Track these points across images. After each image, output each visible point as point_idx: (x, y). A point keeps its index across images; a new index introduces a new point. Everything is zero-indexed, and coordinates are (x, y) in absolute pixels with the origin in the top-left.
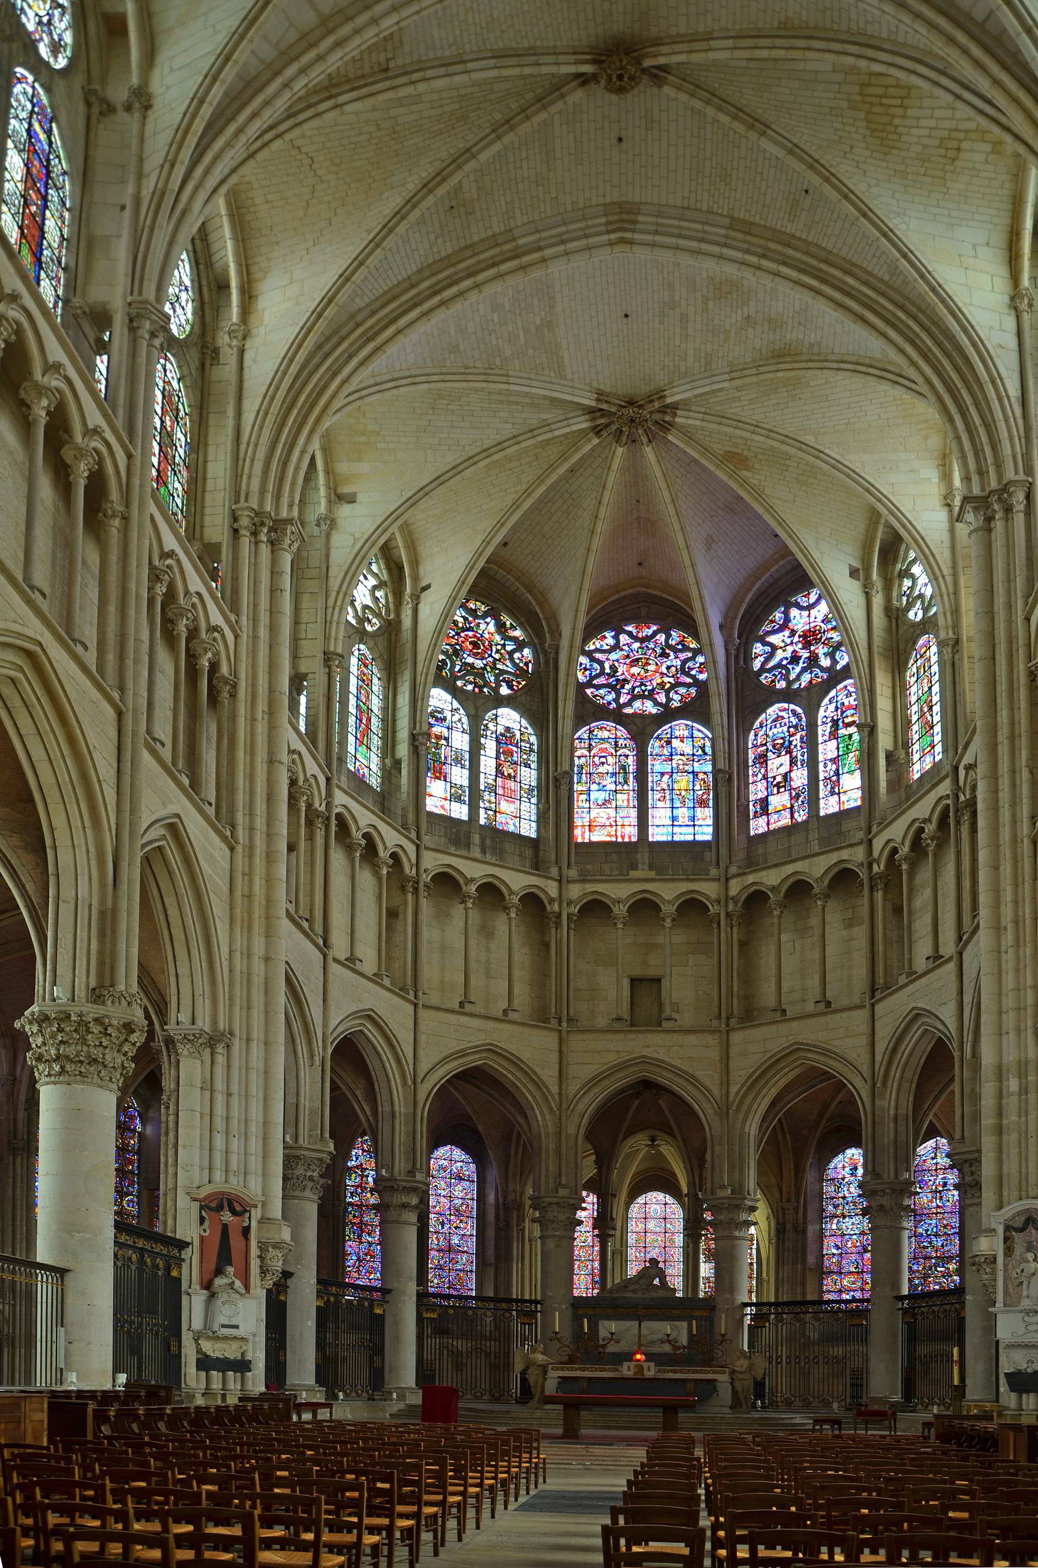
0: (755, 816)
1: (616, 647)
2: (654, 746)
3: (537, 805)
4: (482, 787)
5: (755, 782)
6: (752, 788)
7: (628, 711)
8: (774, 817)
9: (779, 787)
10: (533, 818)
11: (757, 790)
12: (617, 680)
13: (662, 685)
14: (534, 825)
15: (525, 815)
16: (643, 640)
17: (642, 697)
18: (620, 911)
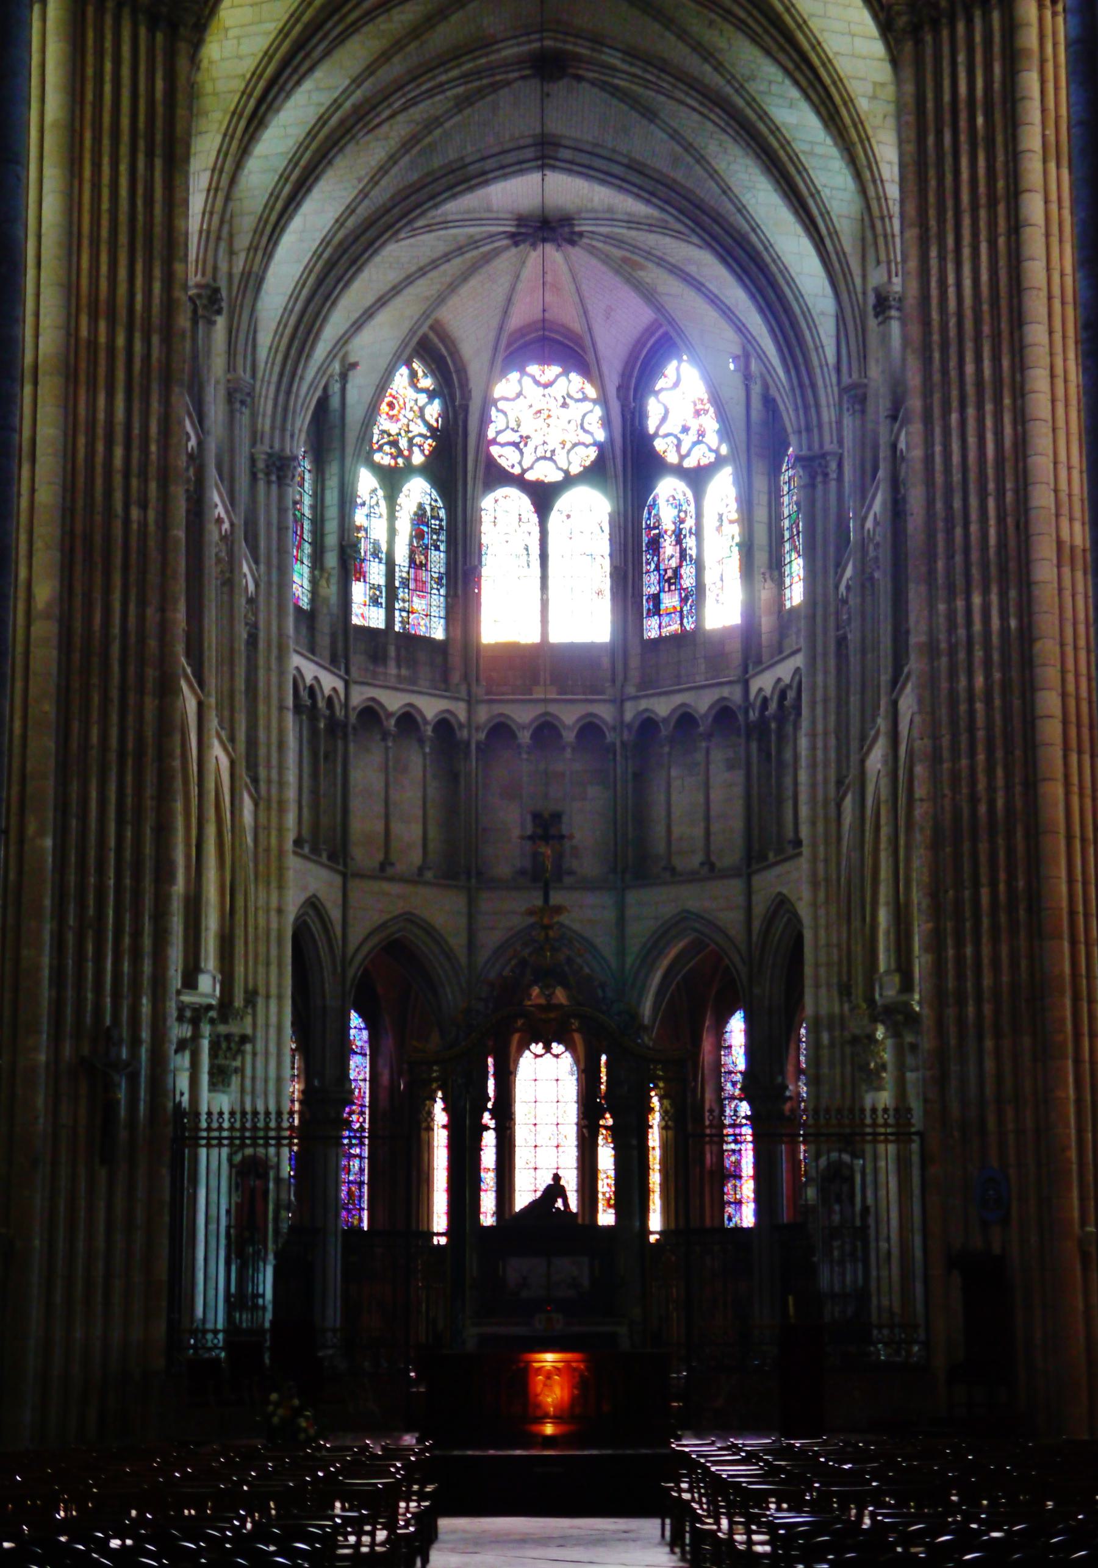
0: (648, 615)
1: (519, 395)
2: (555, 519)
3: (446, 596)
4: (397, 584)
5: (648, 572)
6: (645, 578)
7: (530, 476)
8: (665, 620)
9: (670, 585)
10: (442, 614)
11: (651, 585)
12: (521, 437)
13: (563, 443)
14: (442, 621)
15: (435, 612)
16: (546, 386)
17: (544, 458)
18: (525, 737)
